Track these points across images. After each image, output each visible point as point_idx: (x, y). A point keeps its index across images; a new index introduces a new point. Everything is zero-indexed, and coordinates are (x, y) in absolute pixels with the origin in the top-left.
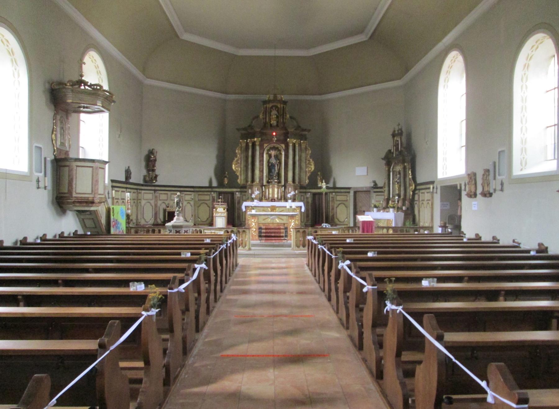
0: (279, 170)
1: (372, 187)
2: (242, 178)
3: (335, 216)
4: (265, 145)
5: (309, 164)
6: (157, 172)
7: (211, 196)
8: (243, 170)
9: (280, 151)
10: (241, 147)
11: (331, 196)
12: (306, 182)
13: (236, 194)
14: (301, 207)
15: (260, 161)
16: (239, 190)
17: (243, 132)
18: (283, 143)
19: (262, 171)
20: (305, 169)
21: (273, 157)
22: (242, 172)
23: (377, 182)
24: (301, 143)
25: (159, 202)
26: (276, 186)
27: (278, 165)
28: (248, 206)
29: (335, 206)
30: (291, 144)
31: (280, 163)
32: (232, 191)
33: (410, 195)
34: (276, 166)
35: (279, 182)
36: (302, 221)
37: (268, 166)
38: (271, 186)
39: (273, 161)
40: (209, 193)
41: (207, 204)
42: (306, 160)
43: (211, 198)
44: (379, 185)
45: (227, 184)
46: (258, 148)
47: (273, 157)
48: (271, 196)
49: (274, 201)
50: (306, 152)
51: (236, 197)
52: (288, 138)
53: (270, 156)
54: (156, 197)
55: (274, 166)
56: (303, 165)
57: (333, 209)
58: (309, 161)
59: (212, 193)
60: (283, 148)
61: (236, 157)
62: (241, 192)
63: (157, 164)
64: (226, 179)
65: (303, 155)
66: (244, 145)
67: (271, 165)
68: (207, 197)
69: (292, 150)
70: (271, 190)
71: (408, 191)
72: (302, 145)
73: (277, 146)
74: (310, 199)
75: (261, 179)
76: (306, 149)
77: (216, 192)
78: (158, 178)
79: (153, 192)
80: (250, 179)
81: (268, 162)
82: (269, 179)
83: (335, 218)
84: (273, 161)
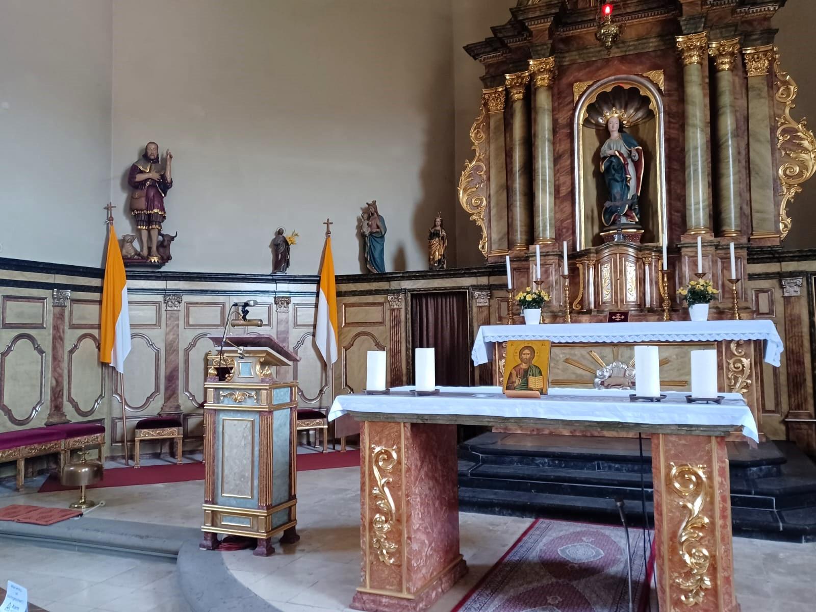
0: (647, 184)
2: (495, 236)
4: (578, 88)
6: (168, 228)
7: (387, 306)
8: (497, 204)
9: (646, 101)
10: (488, 117)
12: (778, 232)
13: (472, 296)
14: (760, 346)
15: (557, 159)
16: (483, 280)
17: (493, 57)
18: (655, 67)
19: (564, 196)
20: (770, 172)
21: (615, 134)
22: (493, 212)
24: (743, 55)
25: (186, 336)
26: (631, 251)
27: (637, 165)
28: (500, 344)
30: (695, 59)
31: (649, 156)
32: (460, 288)
34: (631, 169)
35: (649, 236)
36: (770, 405)
37: (597, 174)
38: (606, 252)
39: (616, 146)
40: (380, 298)
41: (373, 336)
42: (773, 130)
43: (388, 313)
45: (439, 261)
46: (543, 100)
47: (615, 134)
48: (607, 295)
49: (625, 320)
50: (771, 97)
51: (475, 310)
52: (681, 34)
53: (604, 133)
54: (173, 317)
55: (623, 168)
56: (761, 153)
58: (792, 131)
59: (390, 297)
60: (656, 85)
61: (471, 156)
62: (490, 288)
63: (171, 200)
64: (435, 241)
65: (760, 109)
66: (496, 106)
67: (608, 169)
68: (374, 314)
69: (702, 85)
70: (606, 270)
72: (751, 66)
73: (626, 78)
75: (565, 229)
76: (771, 77)
77: (405, 291)
78: (174, 249)
79: (159, 298)
80: (520, 236)
81: (597, 158)
82: (602, 228)
84: (616, 146)
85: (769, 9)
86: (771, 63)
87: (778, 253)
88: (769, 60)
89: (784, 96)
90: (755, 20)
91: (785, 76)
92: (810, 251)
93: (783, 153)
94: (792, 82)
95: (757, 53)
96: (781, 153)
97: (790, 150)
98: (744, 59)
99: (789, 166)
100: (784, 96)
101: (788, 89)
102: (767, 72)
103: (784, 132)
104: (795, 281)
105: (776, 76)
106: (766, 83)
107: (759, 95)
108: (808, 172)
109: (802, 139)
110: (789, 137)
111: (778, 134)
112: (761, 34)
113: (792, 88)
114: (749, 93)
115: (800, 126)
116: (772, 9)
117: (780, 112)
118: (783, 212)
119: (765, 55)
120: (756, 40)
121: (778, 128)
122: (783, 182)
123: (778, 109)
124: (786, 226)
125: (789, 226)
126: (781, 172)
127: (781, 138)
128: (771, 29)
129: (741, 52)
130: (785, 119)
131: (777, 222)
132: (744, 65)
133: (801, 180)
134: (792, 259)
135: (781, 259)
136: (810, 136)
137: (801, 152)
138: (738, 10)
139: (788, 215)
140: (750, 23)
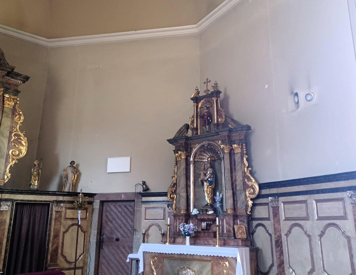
1: (140, 193)
3: (60, 251)
5: (18, 141)
11: (55, 209)
20: (5, 151)
23: (148, 184)
24: (4, 97)
29: (62, 230)
33: (247, 206)
42: (11, 133)
44: (153, 190)
50: (13, 119)
57: (56, 236)
71: (241, 198)
72: (7, 102)
74: (9, 213)
76: (14, 110)
83: (59, 255)
85: (18, 82)
86: (16, 104)
87: (2, 189)
88: (14, 103)
89: (18, 120)
90: (12, 84)
91: (20, 112)
92: (16, 190)
93: (13, 144)
94: (23, 115)
95: (10, 98)
96: (12, 144)
97: (16, 143)
98: (4, 98)
99: (14, 150)
100: (18, 120)
101: (20, 117)
102: (13, 107)
103: (15, 135)
104: (7, 203)
105: (16, 110)
106: (11, 112)
107: (8, 116)
108: (22, 154)
109: (22, 140)
110: (17, 138)
111: (12, 135)
112: (13, 91)
113: (22, 117)
114: (4, 114)
115: (22, 134)
116: (19, 82)
117: (15, 126)
118: (8, 170)
119: (13, 100)
120: (11, 92)
121: (13, 132)
122: (11, 157)
123: (14, 124)
124: (8, 177)
125: (9, 177)
126: (10, 152)
127: (13, 137)
128: (18, 90)
129: (3, 95)
130: (16, 129)
131: (4, 175)
132: (4, 101)
133: (18, 158)
134: (7, 193)
135: (2, 192)
136: (26, 140)
137: (21, 146)
138: (5, 77)
139: (10, 172)
140: (9, 84)
